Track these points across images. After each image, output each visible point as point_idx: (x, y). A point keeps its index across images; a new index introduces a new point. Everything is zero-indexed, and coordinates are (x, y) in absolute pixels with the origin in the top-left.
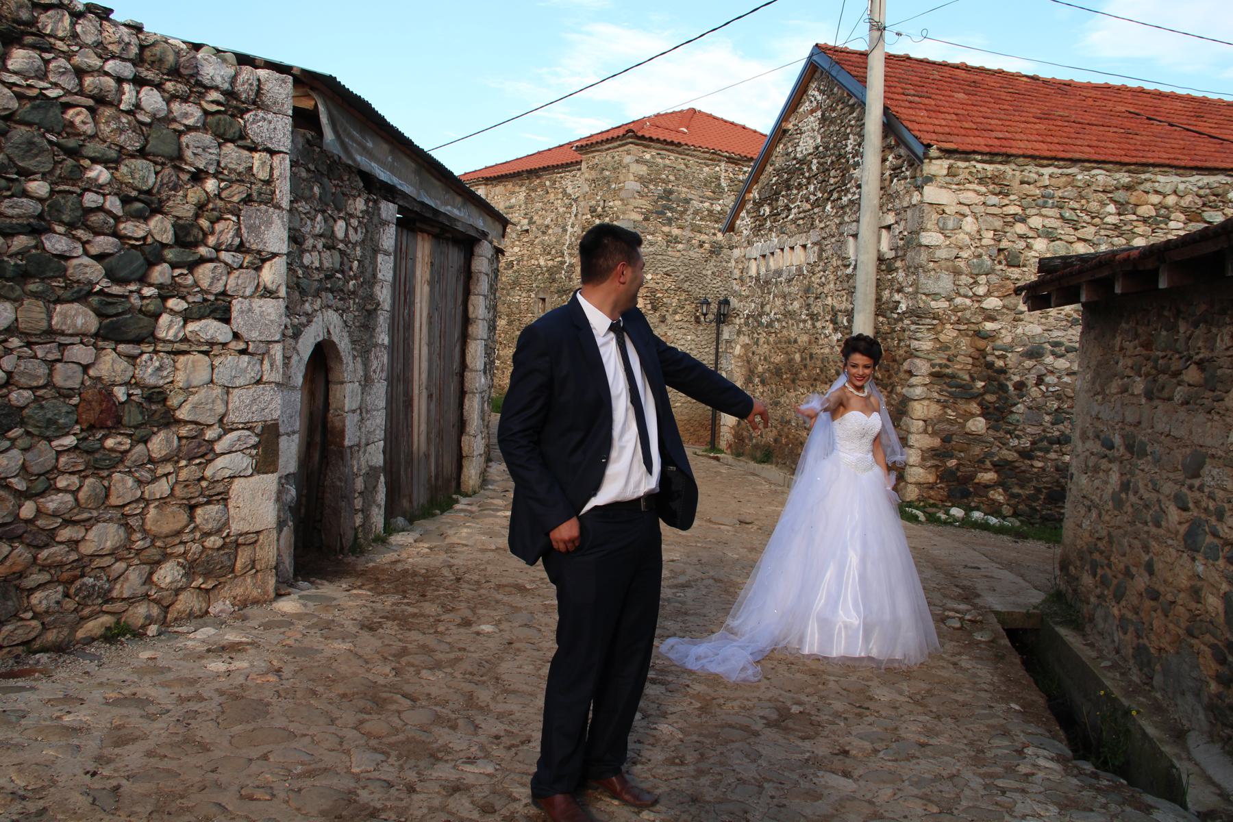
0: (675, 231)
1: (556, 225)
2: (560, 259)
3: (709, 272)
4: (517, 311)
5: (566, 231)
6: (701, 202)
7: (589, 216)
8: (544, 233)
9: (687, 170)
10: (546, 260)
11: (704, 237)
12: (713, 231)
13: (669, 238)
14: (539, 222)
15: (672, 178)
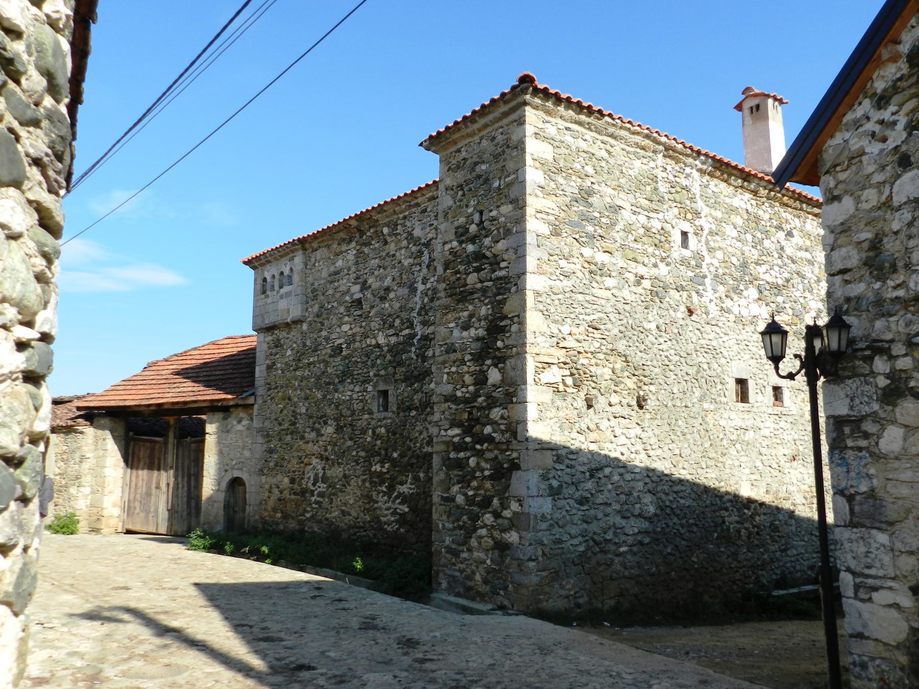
0: (601, 257)
1: (400, 285)
3: (653, 326)
4: (349, 413)
5: (416, 289)
6: (634, 213)
7: (455, 244)
8: (383, 299)
9: (612, 161)
10: (388, 336)
11: (641, 270)
12: (653, 260)
13: (593, 267)
15: (590, 170)
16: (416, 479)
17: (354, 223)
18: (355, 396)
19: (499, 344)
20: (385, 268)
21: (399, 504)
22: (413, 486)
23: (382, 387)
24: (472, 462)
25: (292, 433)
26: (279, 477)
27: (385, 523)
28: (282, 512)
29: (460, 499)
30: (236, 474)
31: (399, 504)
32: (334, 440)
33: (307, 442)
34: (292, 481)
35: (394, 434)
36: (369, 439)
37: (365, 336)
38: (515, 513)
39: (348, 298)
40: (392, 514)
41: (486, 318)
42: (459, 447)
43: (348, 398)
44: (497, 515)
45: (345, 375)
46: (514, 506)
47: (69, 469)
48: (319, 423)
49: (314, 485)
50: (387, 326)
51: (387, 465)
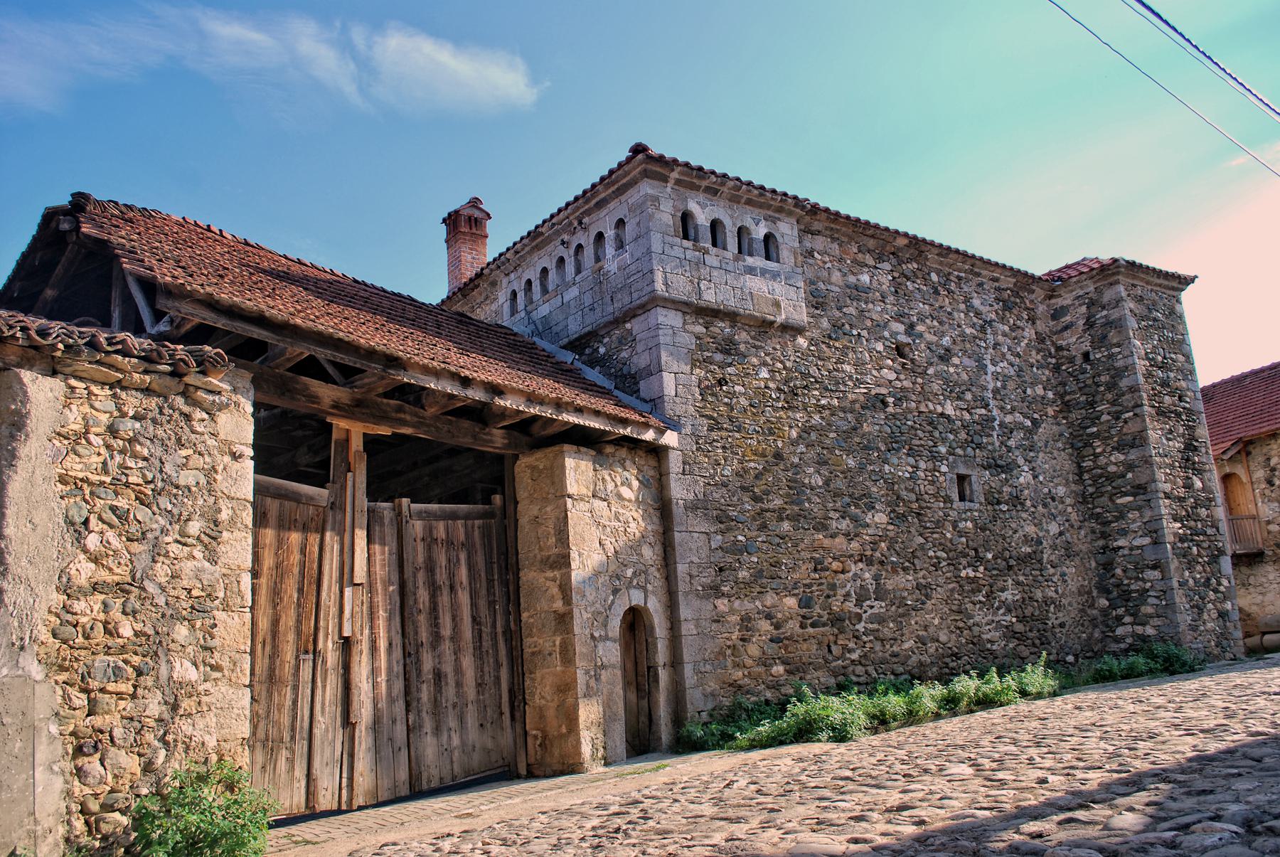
2: (983, 411)
4: (913, 497)
14: (930, 338)
16: (1018, 583)
17: (902, 242)
18: (921, 474)
19: (1196, 459)
20: (940, 323)
21: (1004, 614)
23: (963, 471)
25: (794, 518)
26: (770, 599)
27: (989, 641)
29: (1191, 581)
30: (637, 598)
31: (1004, 614)
32: (891, 534)
33: (833, 536)
34: (805, 603)
37: (925, 395)
38: (1225, 587)
39: (886, 334)
40: (996, 629)
41: (1183, 435)
42: (1182, 539)
43: (908, 475)
44: (1216, 591)
45: (894, 442)
46: (1225, 582)
47: (162, 571)
48: (857, 506)
49: (859, 603)
50: (954, 395)
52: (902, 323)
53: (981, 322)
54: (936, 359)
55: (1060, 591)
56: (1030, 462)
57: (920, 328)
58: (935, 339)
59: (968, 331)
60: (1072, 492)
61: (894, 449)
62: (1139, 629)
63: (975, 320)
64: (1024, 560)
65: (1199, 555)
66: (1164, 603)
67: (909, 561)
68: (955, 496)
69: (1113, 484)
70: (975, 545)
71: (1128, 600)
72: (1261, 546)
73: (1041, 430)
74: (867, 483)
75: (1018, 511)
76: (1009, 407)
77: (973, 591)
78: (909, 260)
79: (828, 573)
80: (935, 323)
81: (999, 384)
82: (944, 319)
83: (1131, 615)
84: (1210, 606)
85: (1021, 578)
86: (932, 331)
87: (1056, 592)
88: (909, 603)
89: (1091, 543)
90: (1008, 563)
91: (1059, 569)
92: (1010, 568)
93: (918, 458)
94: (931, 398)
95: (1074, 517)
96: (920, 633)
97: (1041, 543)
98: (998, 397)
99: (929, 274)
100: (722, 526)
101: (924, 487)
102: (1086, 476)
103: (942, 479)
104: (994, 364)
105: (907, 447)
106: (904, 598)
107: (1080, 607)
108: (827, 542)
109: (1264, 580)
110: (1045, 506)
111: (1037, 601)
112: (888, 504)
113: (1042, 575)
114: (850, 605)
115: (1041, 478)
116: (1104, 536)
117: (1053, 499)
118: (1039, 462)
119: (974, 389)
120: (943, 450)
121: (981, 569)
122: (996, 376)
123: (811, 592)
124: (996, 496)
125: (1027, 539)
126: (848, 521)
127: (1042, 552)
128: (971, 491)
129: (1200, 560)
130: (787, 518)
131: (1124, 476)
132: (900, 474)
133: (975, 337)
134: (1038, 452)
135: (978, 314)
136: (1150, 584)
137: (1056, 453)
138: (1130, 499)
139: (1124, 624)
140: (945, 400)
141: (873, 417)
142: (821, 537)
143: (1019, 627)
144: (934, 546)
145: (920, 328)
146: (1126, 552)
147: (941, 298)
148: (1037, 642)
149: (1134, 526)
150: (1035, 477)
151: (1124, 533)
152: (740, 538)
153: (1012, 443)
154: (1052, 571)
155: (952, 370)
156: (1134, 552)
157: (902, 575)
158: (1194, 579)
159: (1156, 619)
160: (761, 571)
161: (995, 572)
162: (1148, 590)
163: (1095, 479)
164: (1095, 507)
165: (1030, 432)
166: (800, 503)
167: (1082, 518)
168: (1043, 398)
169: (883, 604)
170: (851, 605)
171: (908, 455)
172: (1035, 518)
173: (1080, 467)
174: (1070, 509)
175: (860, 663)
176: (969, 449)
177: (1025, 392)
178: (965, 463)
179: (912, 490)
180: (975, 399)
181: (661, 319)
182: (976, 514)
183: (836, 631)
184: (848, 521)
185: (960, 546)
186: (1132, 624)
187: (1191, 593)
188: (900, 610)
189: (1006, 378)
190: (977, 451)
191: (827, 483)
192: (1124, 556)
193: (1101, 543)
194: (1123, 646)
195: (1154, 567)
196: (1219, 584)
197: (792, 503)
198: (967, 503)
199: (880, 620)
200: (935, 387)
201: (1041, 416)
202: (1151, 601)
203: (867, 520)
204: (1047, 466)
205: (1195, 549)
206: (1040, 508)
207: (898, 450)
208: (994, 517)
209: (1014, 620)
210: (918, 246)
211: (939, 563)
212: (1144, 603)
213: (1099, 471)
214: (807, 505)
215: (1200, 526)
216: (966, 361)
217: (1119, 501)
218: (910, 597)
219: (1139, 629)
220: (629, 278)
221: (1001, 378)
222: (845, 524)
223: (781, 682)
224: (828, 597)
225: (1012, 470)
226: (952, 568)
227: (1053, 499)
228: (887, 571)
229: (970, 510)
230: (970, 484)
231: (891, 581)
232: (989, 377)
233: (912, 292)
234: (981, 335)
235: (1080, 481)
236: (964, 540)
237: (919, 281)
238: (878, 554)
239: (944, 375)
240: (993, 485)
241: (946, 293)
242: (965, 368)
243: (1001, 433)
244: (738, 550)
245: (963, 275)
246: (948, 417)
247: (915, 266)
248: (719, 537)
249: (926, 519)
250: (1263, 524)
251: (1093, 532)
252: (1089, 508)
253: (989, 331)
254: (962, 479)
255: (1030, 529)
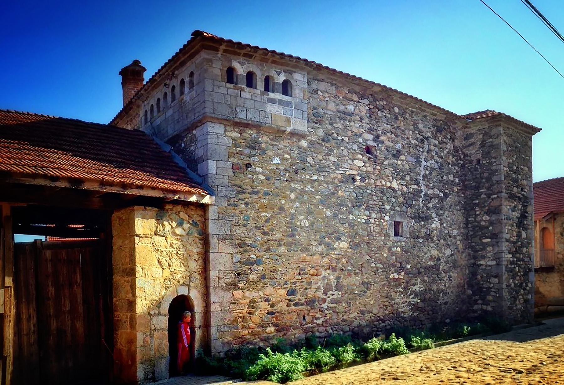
2: (416, 187)
16: (423, 281)
18: (372, 221)
20: (396, 136)
21: (413, 298)
22: (422, 286)
23: (398, 219)
24: (517, 268)
25: (289, 245)
28: (275, 325)
29: (513, 285)
31: (413, 298)
35: (406, 252)
36: (385, 255)
37: (380, 176)
38: (530, 288)
42: (512, 263)
43: (364, 221)
44: (525, 289)
45: (358, 203)
46: (530, 285)
49: (325, 293)
51: (403, 274)
52: (372, 134)
53: (421, 137)
54: (390, 156)
55: (447, 285)
56: (439, 216)
57: (383, 138)
58: (392, 144)
59: (413, 142)
60: (461, 233)
61: (357, 206)
62: (485, 307)
63: (418, 136)
64: (428, 268)
65: (519, 271)
66: (497, 295)
67: (359, 270)
68: (392, 233)
69: (482, 231)
70: (401, 260)
71: (481, 292)
72: (553, 264)
73: (448, 199)
74: (338, 225)
75: (429, 242)
76: (432, 185)
77: (396, 286)
78: (382, 99)
79: (307, 276)
80: (393, 136)
81: (427, 172)
82: (399, 134)
83: (482, 300)
84: (521, 297)
85: (426, 278)
86: (390, 140)
87: (445, 286)
88: (356, 292)
89: (467, 261)
90: (419, 271)
91: (448, 274)
92: (420, 273)
93: (371, 212)
94: (384, 178)
95: (460, 247)
96: (361, 309)
97: (440, 260)
98: (426, 179)
99: (393, 108)
100: (241, 249)
101: (374, 228)
102: (470, 226)
103: (385, 224)
104: (426, 160)
105: (365, 205)
106: (353, 290)
107: (457, 294)
108: (308, 258)
109: (552, 280)
110: (445, 240)
111: (433, 291)
112: (349, 237)
113: (438, 277)
114: (320, 294)
115: (445, 225)
116: (475, 258)
117: (450, 237)
118: (445, 216)
119: (412, 174)
120: (388, 207)
121: (403, 274)
122: (426, 168)
123: (295, 286)
124: (417, 234)
125: (432, 258)
126: (323, 246)
127: (440, 265)
128: (402, 230)
129: (519, 274)
130: (284, 244)
131: (488, 228)
132: (359, 220)
133: (417, 146)
134: (445, 211)
135: (420, 132)
136: (492, 285)
137: (455, 212)
138: (489, 240)
139: (478, 304)
140: (393, 179)
141: (346, 187)
142: (305, 255)
143: (421, 305)
144: (375, 261)
145: (383, 138)
146: (484, 267)
147: (399, 122)
148: (431, 312)
149: (489, 255)
150: (441, 224)
151: (484, 257)
152: (252, 256)
153: (430, 205)
154: (444, 275)
155: (399, 163)
156: (487, 268)
157: (354, 276)
158: (514, 283)
159: (493, 303)
160: (264, 275)
161: (410, 275)
162: (491, 288)
163: (474, 227)
164: (471, 243)
165: (441, 200)
166: (293, 236)
167: (464, 248)
168: (452, 182)
169: (340, 293)
170: (320, 293)
171: (366, 209)
172: (438, 246)
173: (467, 220)
174: (458, 242)
175: (323, 325)
176: (404, 207)
177: (442, 178)
178: (400, 215)
179: (366, 230)
180: (412, 179)
181: (209, 129)
182: (403, 243)
183: (309, 308)
184: (323, 246)
185: (391, 261)
186: (481, 304)
187: (512, 291)
188: (350, 296)
189: (432, 169)
190: (409, 209)
191: (312, 225)
192: (482, 269)
193: (472, 261)
194: (476, 315)
195: (496, 277)
196: (527, 286)
197: (288, 236)
198: (399, 238)
199: (337, 301)
200: (388, 172)
201: (449, 191)
202: (492, 293)
203: (335, 246)
204: (449, 219)
205: (517, 268)
206: (442, 241)
207: (360, 206)
208: (414, 245)
209: (419, 301)
210: (387, 92)
211: (378, 270)
212: (489, 294)
213: (476, 224)
214: (297, 237)
215: (521, 257)
216: (409, 158)
217: (484, 241)
218: (357, 289)
219: (485, 307)
220: (194, 105)
221: (429, 169)
222: (321, 248)
223: (269, 338)
224: (306, 289)
225: (428, 220)
226: (385, 273)
227: (450, 237)
228: (344, 275)
229: (400, 241)
230: (402, 227)
231: (346, 281)
232: (422, 168)
233: (380, 117)
234: (420, 145)
235: (466, 227)
236: (394, 257)
237: (386, 112)
238: (340, 265)
239: (395, 165)
240: (416, 228)
241: (403, 119)
242: (408, 162)
243: (424, 199)
244: (250, 263)
245: (415, 110)
246: (394, 190)
247: (385, 103)
248: (239, 256)
249: (372, 246)
250: (556, 254)
251: (469, 255)
252: (469, 243)
253: (426, 142)
254: (397, 225)
255: (435, 253)
